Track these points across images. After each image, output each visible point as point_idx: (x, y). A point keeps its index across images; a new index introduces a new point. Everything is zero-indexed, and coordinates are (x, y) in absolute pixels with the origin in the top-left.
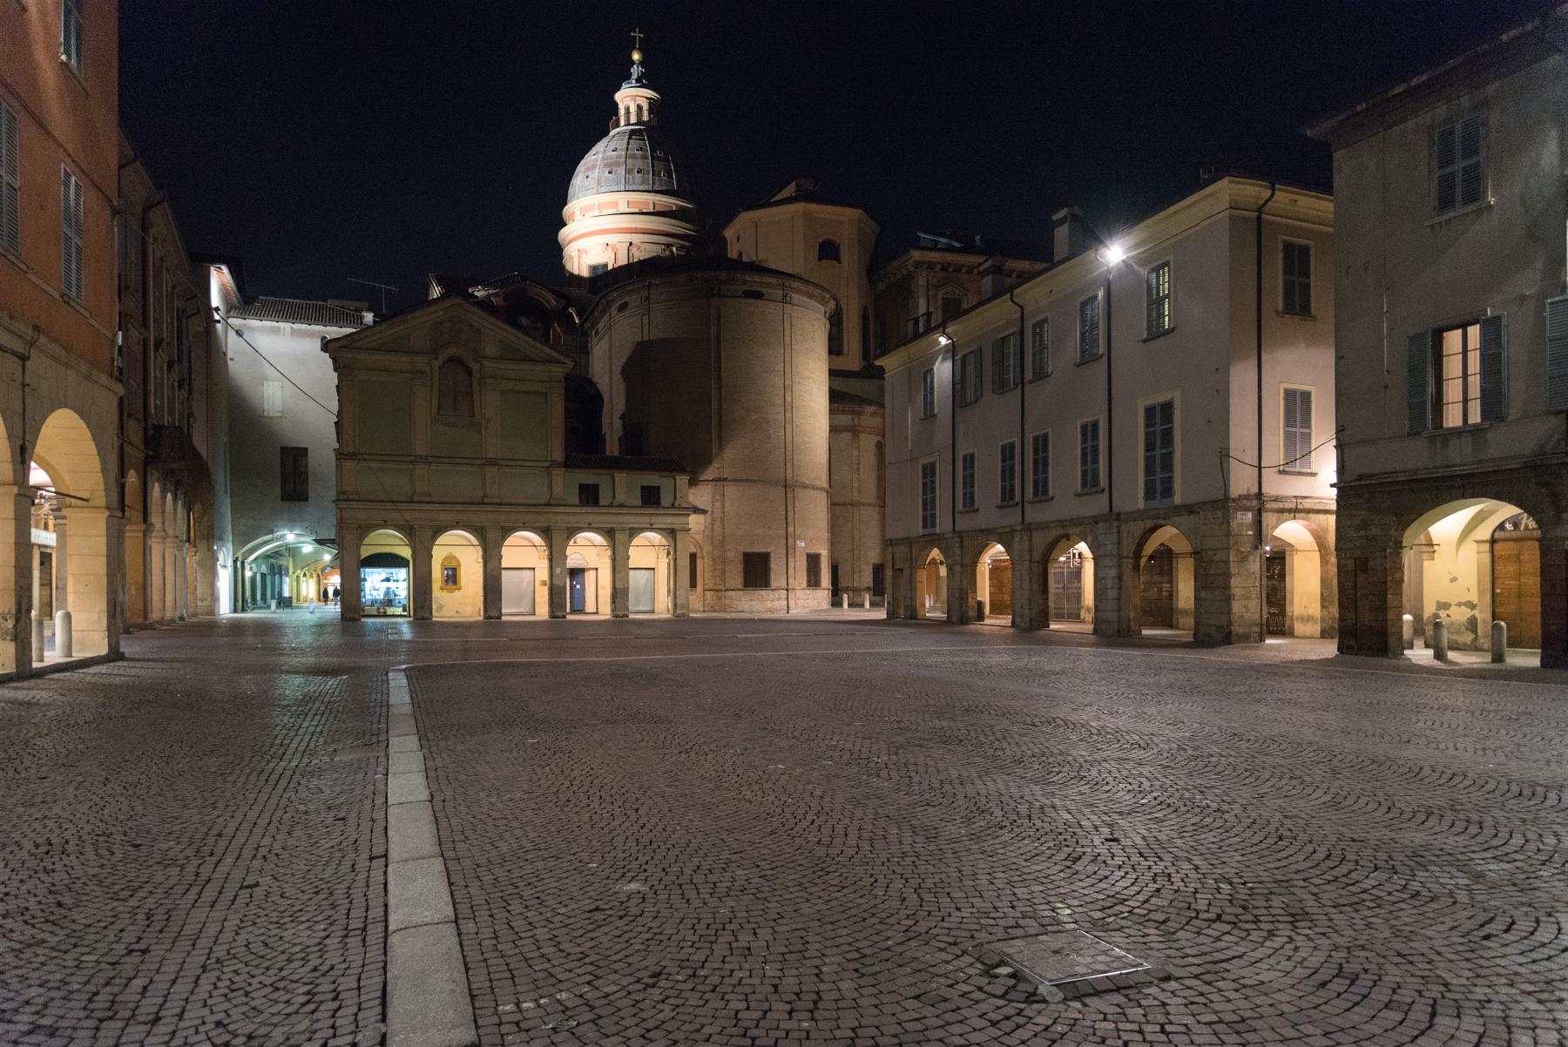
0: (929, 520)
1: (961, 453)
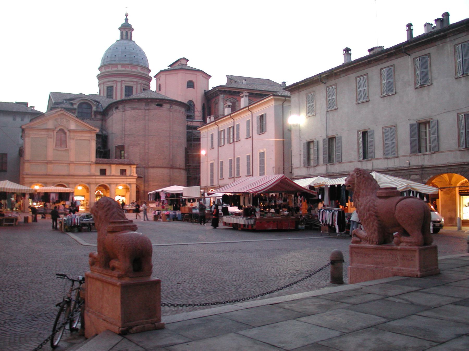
0: (212, 181)
1: (220, 161)
